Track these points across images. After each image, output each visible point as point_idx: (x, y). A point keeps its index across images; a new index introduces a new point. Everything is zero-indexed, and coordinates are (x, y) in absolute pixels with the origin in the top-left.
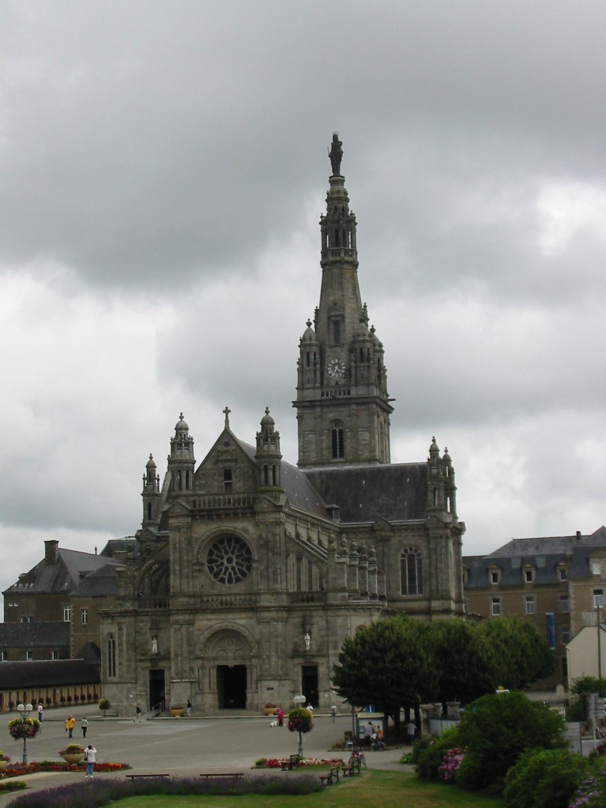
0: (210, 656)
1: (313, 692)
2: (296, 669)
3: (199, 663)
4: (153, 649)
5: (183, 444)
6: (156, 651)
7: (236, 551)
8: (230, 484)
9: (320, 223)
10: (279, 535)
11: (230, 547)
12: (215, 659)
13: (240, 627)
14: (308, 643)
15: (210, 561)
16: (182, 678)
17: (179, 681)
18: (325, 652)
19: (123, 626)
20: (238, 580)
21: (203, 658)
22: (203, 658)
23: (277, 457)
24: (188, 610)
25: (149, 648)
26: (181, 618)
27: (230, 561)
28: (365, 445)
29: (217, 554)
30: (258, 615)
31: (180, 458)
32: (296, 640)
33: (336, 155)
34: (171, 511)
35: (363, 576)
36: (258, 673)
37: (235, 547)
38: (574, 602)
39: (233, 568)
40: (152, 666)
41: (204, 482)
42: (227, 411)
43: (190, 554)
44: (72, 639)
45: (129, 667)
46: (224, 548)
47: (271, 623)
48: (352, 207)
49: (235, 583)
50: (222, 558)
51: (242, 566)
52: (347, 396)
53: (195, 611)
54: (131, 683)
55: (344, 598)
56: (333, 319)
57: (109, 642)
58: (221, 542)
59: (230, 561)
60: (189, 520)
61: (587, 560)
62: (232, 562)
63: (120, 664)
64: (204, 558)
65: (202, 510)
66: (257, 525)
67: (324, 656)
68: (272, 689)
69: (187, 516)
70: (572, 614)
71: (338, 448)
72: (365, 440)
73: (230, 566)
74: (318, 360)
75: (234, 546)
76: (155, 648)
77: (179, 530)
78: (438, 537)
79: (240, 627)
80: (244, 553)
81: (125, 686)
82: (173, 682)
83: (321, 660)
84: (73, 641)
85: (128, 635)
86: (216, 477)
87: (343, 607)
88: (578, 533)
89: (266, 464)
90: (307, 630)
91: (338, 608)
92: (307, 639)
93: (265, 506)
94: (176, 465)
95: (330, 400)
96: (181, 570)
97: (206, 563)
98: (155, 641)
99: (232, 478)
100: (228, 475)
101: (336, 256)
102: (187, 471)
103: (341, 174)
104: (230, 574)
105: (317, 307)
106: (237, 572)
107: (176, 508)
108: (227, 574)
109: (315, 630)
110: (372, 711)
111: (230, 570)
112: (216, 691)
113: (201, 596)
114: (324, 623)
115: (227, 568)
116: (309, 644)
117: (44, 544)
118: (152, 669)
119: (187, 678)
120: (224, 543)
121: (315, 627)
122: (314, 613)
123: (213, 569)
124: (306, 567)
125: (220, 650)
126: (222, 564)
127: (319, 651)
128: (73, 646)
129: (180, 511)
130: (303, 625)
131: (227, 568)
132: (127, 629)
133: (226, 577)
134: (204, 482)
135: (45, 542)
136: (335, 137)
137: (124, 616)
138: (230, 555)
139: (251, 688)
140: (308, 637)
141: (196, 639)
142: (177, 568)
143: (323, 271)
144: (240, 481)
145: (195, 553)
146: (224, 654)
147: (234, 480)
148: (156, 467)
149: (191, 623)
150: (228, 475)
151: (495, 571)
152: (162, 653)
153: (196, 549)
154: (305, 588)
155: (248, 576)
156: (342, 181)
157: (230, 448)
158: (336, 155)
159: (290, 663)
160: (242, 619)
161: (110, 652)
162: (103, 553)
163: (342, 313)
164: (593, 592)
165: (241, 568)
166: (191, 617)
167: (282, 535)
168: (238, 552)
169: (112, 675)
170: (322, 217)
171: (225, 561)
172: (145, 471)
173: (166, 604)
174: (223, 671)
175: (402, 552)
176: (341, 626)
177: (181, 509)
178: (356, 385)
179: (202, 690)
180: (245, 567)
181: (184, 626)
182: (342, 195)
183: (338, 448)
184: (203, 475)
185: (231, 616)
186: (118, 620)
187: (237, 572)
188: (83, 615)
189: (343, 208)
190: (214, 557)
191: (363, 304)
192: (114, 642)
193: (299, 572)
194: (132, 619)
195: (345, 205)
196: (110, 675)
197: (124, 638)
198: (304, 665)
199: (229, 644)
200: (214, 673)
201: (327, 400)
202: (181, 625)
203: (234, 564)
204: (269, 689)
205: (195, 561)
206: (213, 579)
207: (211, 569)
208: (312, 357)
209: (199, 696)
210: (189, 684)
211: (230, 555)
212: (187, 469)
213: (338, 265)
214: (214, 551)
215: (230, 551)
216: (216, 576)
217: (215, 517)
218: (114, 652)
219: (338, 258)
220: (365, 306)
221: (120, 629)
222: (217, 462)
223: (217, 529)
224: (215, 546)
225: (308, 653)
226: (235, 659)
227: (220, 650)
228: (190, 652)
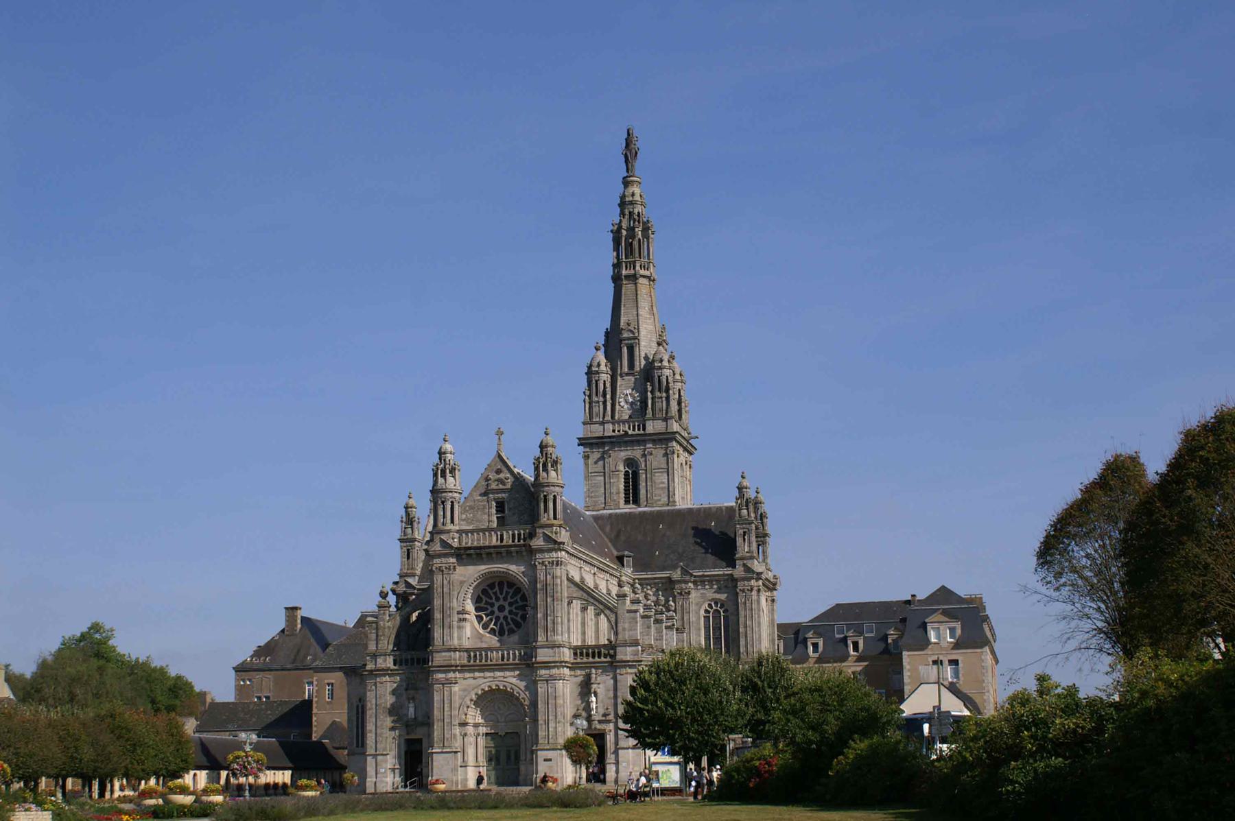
1: (582, 519)
5: (448, 471)
6: (413, 717)
7: (509, 597)
10: (561, 577)
13: (513, 687)
14: (594, 705)
17: (440, 750)
28: (662, 488)
33: (630, 153)
35: (659, 632)
37: (507, 593)
38: (909, 674)
39: (505, 618)
40: (408, 734)
41: (471, 515)
42: (500, 433)
46: (495, 593)
49: (508, 634)
51: (516, 614)
52: (642, 432)
55: (636, 654)
56: (626, 342)
57: (358, 707)
59: (501, 609)
65: (469, 548)
68: (550, 760)
71: (633, 494)
72: (663, 483)
74: (609, 390)
75: (507, 592)
76: (411, 710)
79: (513, 687)
80: (519, 600)
84: (315, 721)
88: (913, 596)
95: (622, 436)
98: (411, 705)
102: (452, 502)
104: (501, 624)
105: (607, 329)
106: (511, 622)
110: (668, 754)
116: (594, 708)
117: (284, 610)
118: (407, 737)
120: (495, 587)
123: (482, 618)
124: (591, 619)
125: (491, 714)
127: (605, 715)
134: (471, 515)
139: (525, 760)
140: (594, 699)
143: (614, 287)
144: (514, 514)
151: (815, 641)
152: (420, 719)
154: (591, 641)
155: (523, 626)
158: (630, 153)
161: (358, 718)
162: (354, 627)
163: (637, 335)
165: (515, 617)
167: (564, 578)
173: (426, 661)
175: (706, 606)
178: (654, 418)
180: (519, 616)
183: (633, 494)
189: (639, 213)
193: (583, 624)
195: (640, 211)
196: (357, 746)
201: (618, 436)
203: (506, 613)
204: (545, 760)
206: (481, 631)
207: (479, 618)
211: (501, 602)
224: (484, 592)
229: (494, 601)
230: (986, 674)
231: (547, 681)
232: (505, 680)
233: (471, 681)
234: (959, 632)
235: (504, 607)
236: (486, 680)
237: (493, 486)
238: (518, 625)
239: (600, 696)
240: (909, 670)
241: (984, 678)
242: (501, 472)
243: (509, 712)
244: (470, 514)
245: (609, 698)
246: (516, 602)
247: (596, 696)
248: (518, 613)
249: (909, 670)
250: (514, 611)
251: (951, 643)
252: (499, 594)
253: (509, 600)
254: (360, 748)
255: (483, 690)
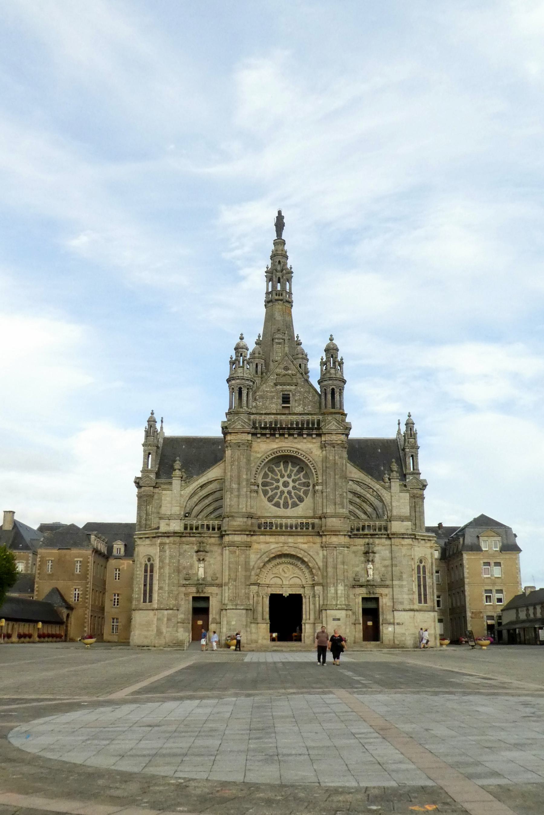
0: (264, 582)
2: (357, 600)
3: (254, 588)
4: (200, 573)
7: (293, 475)
8: (289, 407)
9: (266, 272)
11: (286, 471)
12: (268, 586)
14: (371, 572)
15: (265, 484)
16: (236, 605)
17: (234, 607)
18: (388, 582)
19: (167, 547)
20: (295, 505)
21: (258, 585)
22: (258, 585)
23: (343, 382)
24: (245, 531)
25: (194, 572)
26: (237, 538)
27: (286, 484)
29: (272, 477)
30: (324, 539)
31: (242, 375)
32: (357, 569)
33: (280, 224)
34: (232, 427)
36: (321, 603)
37: (291, 471)
38: (468, 571)
39: (289, 493)
41: (261, 403)
43: (249, 473)
44: (36, 586)
45: (170, 592)
46: (280, 471)
47: (337, 548)
48: (290, 263)
50: (278, 481)
51: (299, 490)
53: (252, 533)
54: (172, 609)
56: (277, 341)
57: (146, 565)
58: (277, 464)
59: (286, 484)
60: (249, 437)
61: (478, 537)
62: (288, 486)
63: (160, 588)
64: (260, 481)
66: (323, 447)
67: (387, 586)
68: (339, 620)
69: (248, 433)
70: (466, 581)
73: (286, 490)
77: (239, 446)
78: (417, 497)
80: (302, 478)
81: (166, 612)
82: (226, 610)
83: (384, 591)
84: (37, 587)
85: (171, 557)
86: (274, 400)
87: (407, 537)
89: (333, 387)
90: (371, 559)
91: (403, 536)
92: (371, 568)
93: (334, 427)
94: (238, 381)
96: (239, 490)
97: (260, 485)
99: (291, 402)
100: (286, 399)
101: (279, 296)
102: (248, 389)
103: (283, 238)
104: (286, 497)
105: (259, 334)
106: (294, 496)
107: (237, 423)
108: (283, 497)
109: (377, 557)
111: (286, 494)
112: (268, 621)
113: (259, 518)
114: (387, 553)
115: (282, 492)
116: (372, 574)
117: (3, 513)
119: (242, 605)
121: (377, 555)
122: (377, 541)
123: (268, 492)
125: (274, 577)
126: (277, 488)
128: (37, 591)
129: (241, 427)
130: (366, 553)
131: (282, 492)
132: (170, 551)
133: (282, 502)
134: (261, 403)
135: (5, 512)
136: (280, 212)
137: (168, 537)
138: (286, 479)
141: (252, 564)
142: (235, 486)
144: (299, 405)
145: (254, 473)
146: (279, 581)
147: (292, 404)
148: (156, 422)
149: (249, 546)
150: (286, 399)
152: (209, 579)
153: (254, 469)
156: (284, 243)
157: (290, 372)
158: (280, 224)
159: (352, 592)
160: (304, 543)
161: (146, 576)
164: (482, 564)
166: (249, 539)
168: (295, 475)
169: (148, 601)
170: (267, 268)
171: (280, 484)
172: (146, 424)
174: (275, 599)
176: (404, 556)
177: (242, 425)
179: (256, 619)
181: (239, 548)
182: (284, 253)
184: (261, 397)
185: (291, 540)
186: (159, 541)
187: (294, 496)
188: (49, 565)
190: (268, 480)
191: (296, 335)
192: (152, 566)
194: (177, 539)
196: (145, 601)
197: (167, 561)
198: (365, 596)
199: (283, 570)
200: (267, 601)
202: (238, 547)
203: (290, 488)
204: (334, 620)
205: (253, 481)
207: (265, 493)
208: (259, 367)
209: (253, 625)
210: (244, 611)
211: (286, 479)
212: (249, 387)
213: (280, 302)
214: (269, 473)
215: (286, 474)
216: (270, 500)
217: (277, 436)
218: (151, 576)
219: (281, 298)
220: (298, 337)
221: (162, 550)
222: (276, 385)
223: (278, 449)
225: (372, 583)
226: (291, 586)
227: (274, 577)
228: (248, 577)
229: (279, 477)
230: (519, 573)
231: (335, 547)
232: (295, 545)
233: (263, 547)
234: (499, 545)
235: (288, 483)
236: (276, 546)
237: (283, 380)
238: (301, 500)
239: (377, 565)
240: (468, 568)
241: (518, 576)
242: (288, 369)
243: (292, 576)
244: (260, 402)
245: (388, 566)
246: (299, 479)
247: (373, 565)
248: (301, 489)
249: (468, 568)
250: (297, 486)
251: (496, 551)
252: (283, 472)
253: (293, 477)
254: (148, 603)
255: (272, 553)
